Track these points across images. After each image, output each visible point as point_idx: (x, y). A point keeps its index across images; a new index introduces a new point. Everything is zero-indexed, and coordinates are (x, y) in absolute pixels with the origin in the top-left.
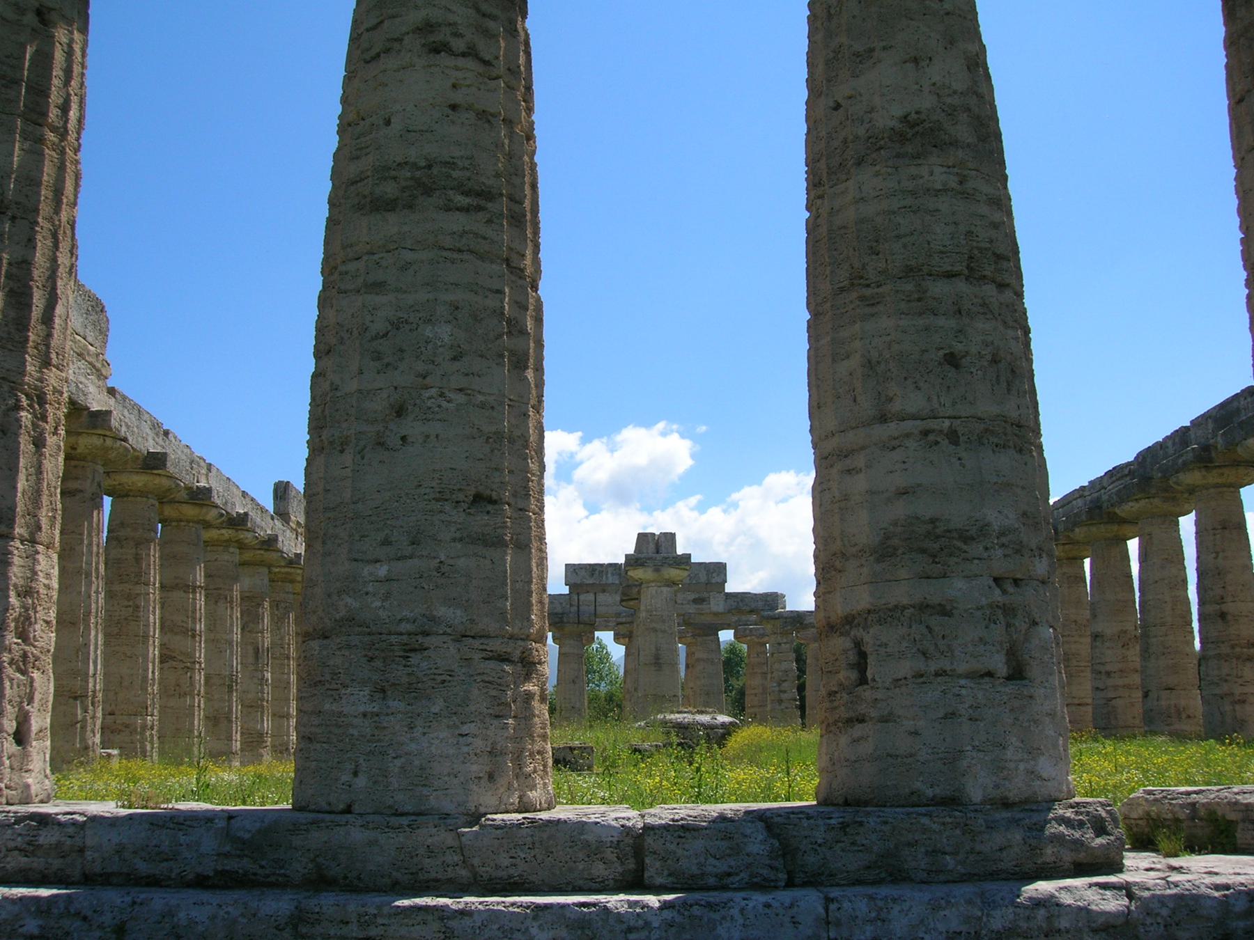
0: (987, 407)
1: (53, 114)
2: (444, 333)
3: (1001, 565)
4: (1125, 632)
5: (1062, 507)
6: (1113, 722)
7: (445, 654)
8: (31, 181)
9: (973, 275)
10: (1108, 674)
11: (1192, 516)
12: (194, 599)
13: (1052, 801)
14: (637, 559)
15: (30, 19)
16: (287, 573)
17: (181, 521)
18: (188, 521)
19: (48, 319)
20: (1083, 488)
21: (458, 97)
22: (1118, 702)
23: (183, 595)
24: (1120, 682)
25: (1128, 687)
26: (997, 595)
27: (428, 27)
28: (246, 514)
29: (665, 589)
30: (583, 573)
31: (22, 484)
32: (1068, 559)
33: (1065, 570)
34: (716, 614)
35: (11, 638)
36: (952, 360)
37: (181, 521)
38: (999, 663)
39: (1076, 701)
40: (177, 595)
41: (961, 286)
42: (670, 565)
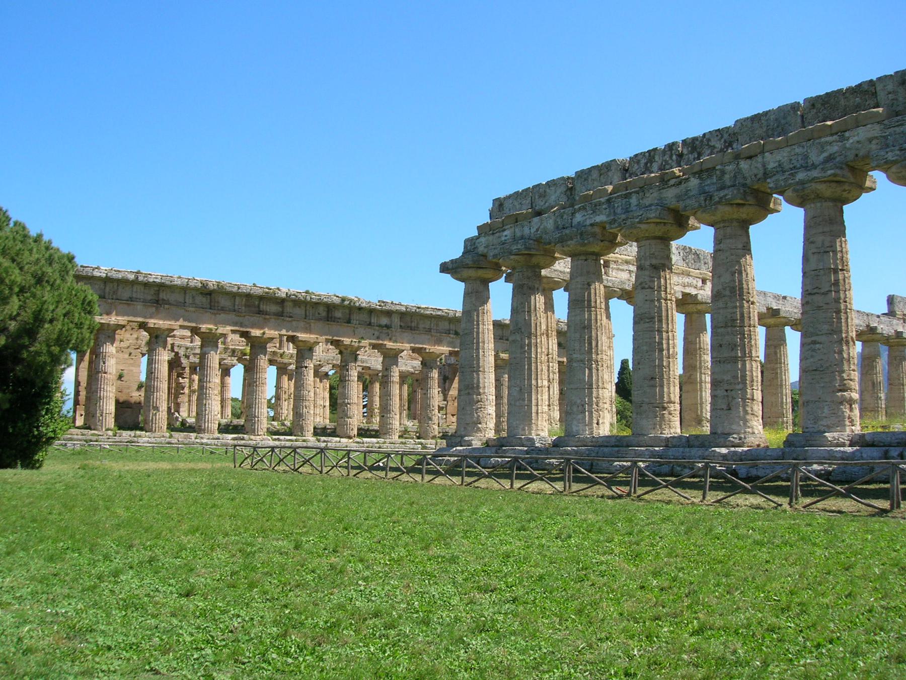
0: (726, 355)
1: (593, 304)
2: (645, 348)
3: (726, 387)
7: (645, 407)
8: (590, 320)
9: (726, 326)
13: (729, 434)
15: (586, 286)
19: (597, 346)
21: (647, 298)
26: (725, 393)
27: (641, 284)
31: (594, 378)
35: (594, 406)
36: (721, 346)
38: (724, 407)
41: (722, 329)
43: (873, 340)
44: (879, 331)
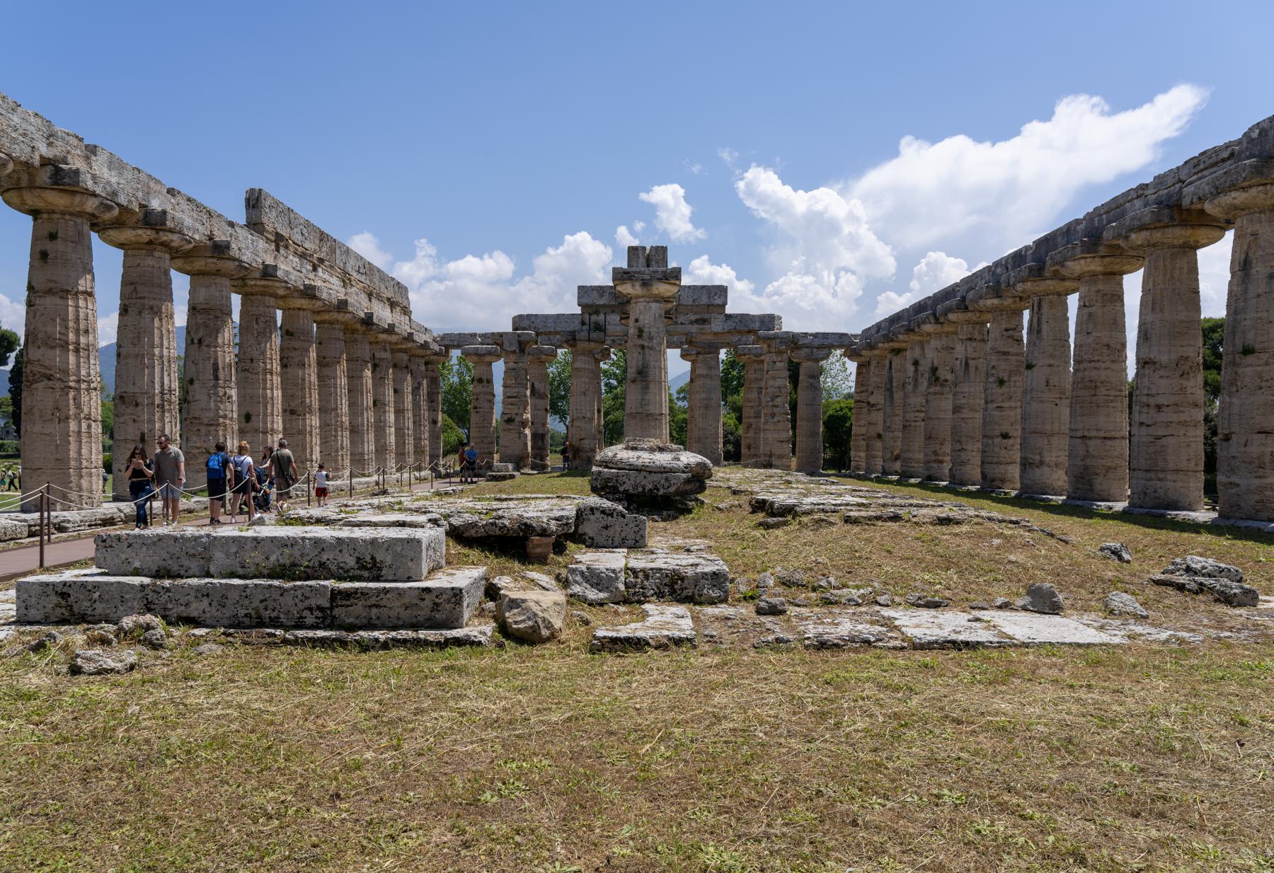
4: (1187, 358)
5: (1107, 213)
6: (1161, 463)
10: (1159, 407)
11: (1232, 231)
12: (77, 307)
14: (626, 272)
16: (264, 286)
17: (53, 212)
18: (63, 213)
20: (1144, 187)
22: (1163, 441)
23: (59, 301)
24: (1175, 417)
25: (1184, 424)
28: (164, 212)
29: (654, 305)
30: (595, 294)
32: (1105, 274)
33: (1101, 287)
34: (716, 334)
37: (53, 212)
39: (1102, 434)
40: (49, 301)
42: (659, 280)
43: (218, 273)
44: (234, 252)
